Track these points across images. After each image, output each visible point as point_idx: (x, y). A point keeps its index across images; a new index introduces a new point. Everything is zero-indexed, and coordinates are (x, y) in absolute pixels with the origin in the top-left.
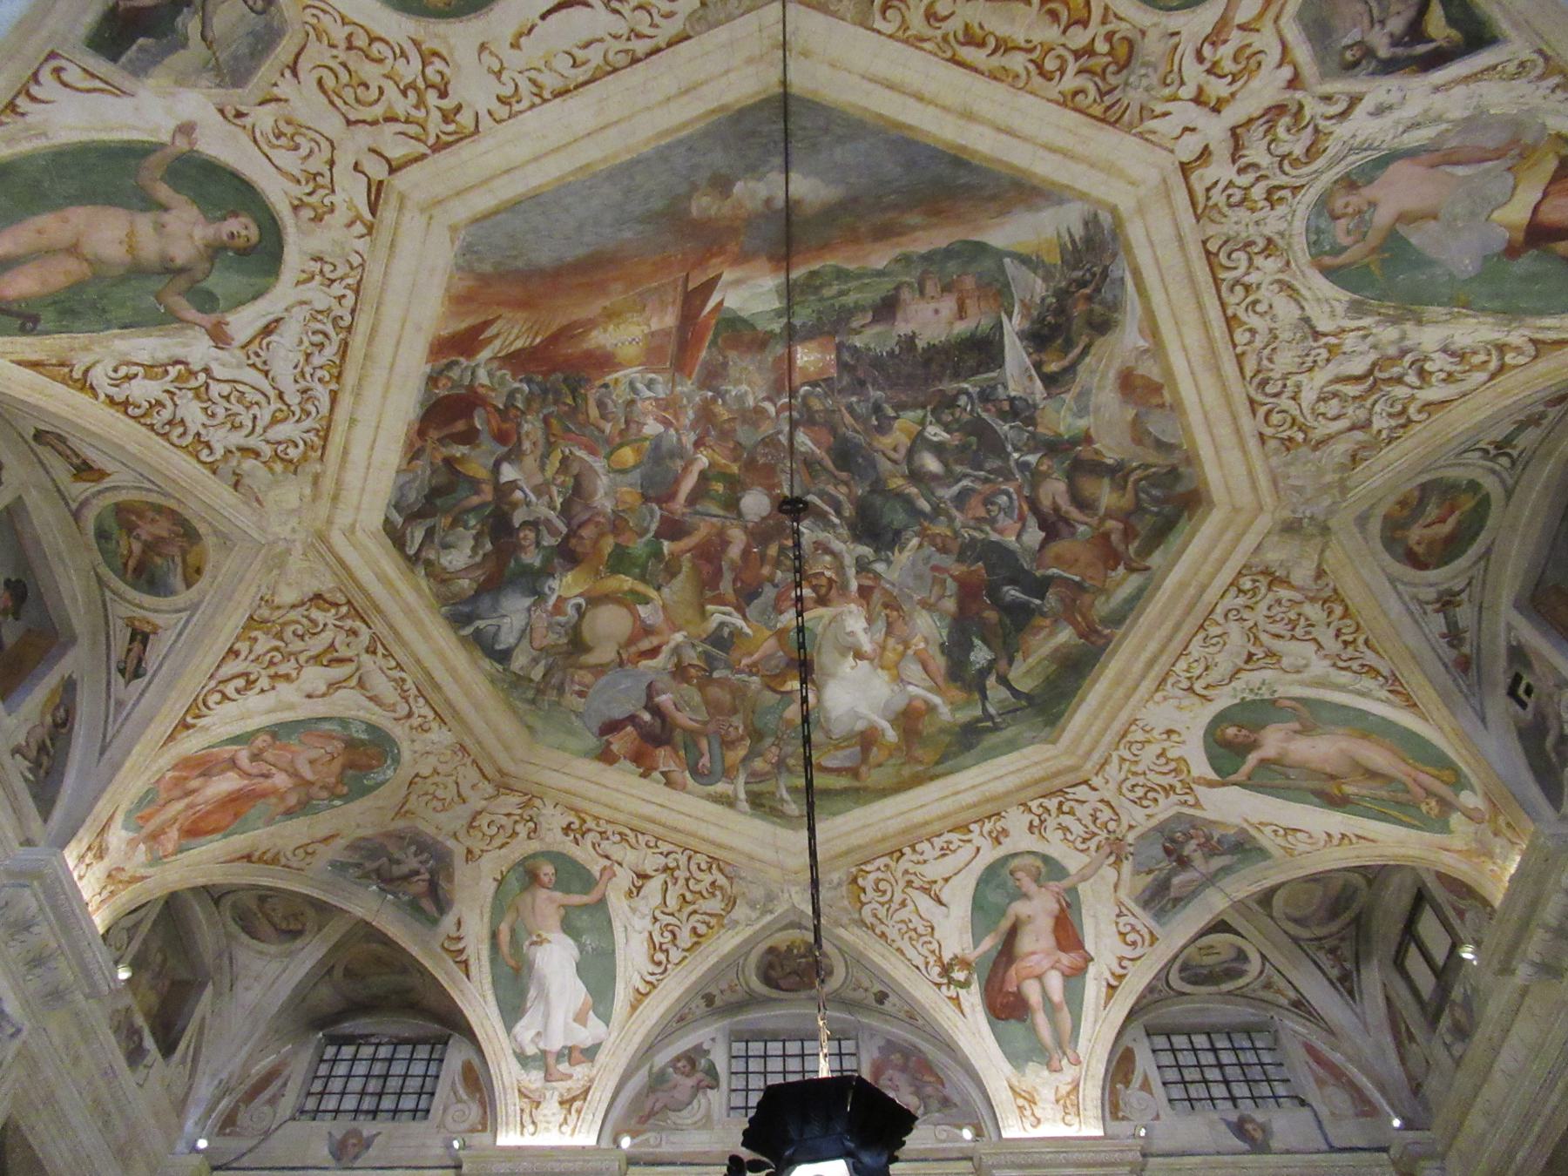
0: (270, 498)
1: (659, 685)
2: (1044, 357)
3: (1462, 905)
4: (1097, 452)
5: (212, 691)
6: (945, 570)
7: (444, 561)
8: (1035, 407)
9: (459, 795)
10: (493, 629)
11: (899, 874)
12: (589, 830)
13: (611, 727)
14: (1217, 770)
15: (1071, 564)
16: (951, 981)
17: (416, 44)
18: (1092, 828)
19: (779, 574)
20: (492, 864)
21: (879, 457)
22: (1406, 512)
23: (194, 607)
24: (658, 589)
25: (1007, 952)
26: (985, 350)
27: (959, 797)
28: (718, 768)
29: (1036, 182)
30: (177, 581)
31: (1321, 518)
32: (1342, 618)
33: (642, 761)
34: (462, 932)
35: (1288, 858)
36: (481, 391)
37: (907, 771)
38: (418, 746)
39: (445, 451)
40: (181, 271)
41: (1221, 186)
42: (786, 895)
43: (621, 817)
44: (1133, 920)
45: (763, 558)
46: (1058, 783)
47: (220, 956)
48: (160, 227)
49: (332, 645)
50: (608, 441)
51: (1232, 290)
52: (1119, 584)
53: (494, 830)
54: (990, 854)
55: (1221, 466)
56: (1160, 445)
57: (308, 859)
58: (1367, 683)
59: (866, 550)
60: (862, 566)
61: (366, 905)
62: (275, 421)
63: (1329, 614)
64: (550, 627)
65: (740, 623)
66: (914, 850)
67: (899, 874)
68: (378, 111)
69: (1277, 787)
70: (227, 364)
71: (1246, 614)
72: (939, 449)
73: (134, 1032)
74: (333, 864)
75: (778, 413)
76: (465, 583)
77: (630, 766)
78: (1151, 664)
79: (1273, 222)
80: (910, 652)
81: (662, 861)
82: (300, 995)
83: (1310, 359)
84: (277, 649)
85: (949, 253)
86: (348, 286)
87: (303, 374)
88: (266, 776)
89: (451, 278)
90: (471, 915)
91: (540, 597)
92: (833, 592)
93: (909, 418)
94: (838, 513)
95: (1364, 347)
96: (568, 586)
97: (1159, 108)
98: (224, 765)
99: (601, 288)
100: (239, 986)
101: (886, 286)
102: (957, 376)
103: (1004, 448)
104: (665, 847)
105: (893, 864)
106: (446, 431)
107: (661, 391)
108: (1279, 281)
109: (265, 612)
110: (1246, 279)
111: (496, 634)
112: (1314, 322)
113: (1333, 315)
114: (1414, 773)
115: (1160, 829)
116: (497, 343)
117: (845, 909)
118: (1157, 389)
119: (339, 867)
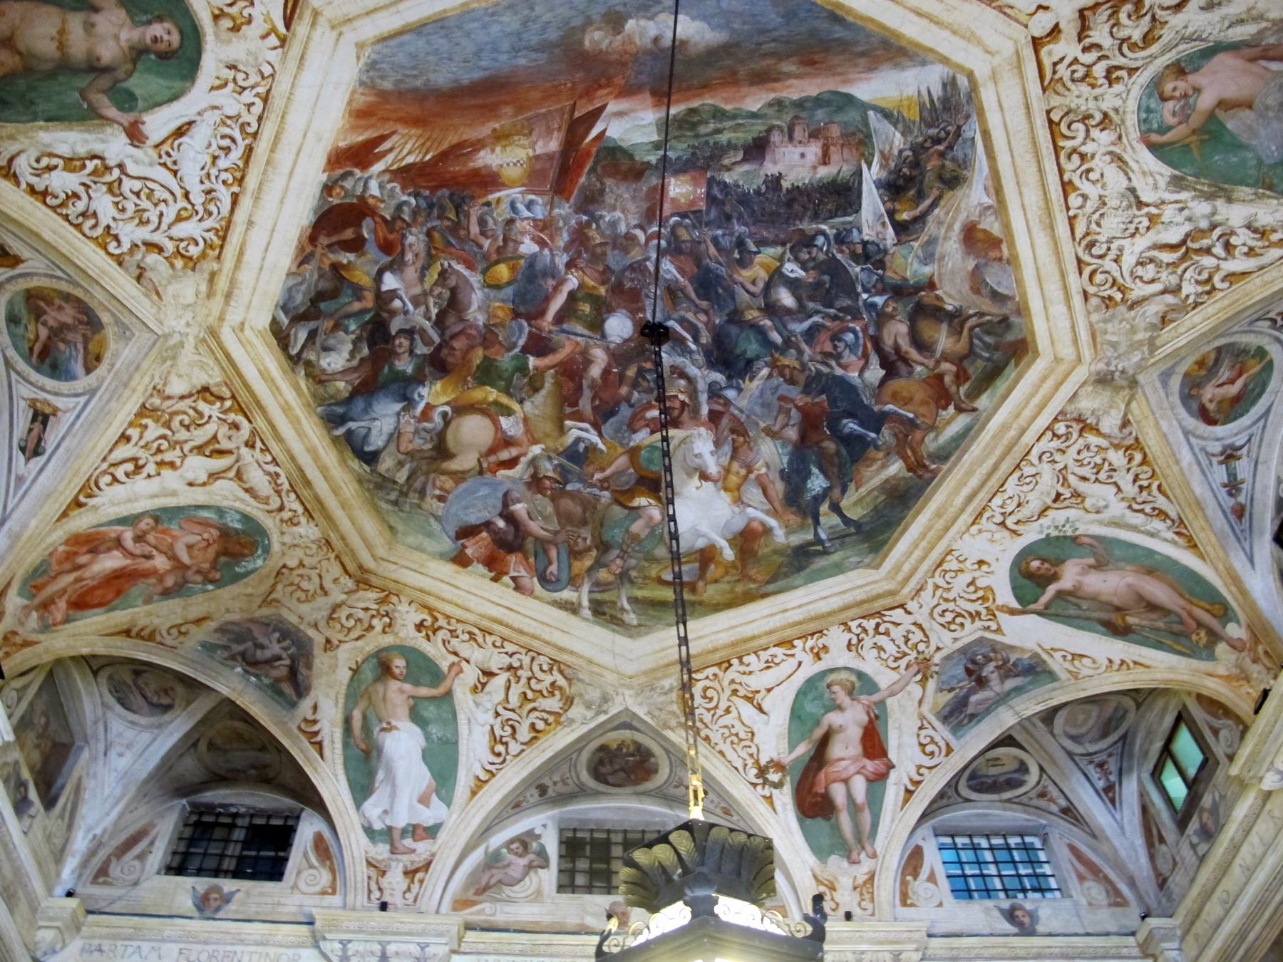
0: (169, 291)
1: (515, 495)
2: (898, 206)
3: (1217, 723)
4: (938, 298)
5: (105, 472)
6: (792, 401)
7: (323, 363)
8: (886, 252)
9: (322, 587)
10: (364, 431)
11: (725, 683)
12: (440, 628)
15: (907, 402)
16: (766, 782)
18: (904, 648)
19: (636, 394)
20: (348, 654)
21: (738, 288)
22: (1203, 373)
23: (92, 392)
24: (521, 402)
26: (843, 195)
28: (565, 577)
29: (904, 43)
30: (78, 368)
31: (1131, 372)
32: (1141, 464)
33: (495, 567)
34: (318, 716)
36: (371, 201)
37: (739, 588)
38: (287, 539)
39: (333, 257)
41: (1066, 62)
42: (620, 698)
44: (930, 732)
45: (621, 378)
46: (877, 605)
47: (96, 723)
49: (215, 437)
50: (486, 257)
51: (1069, 157)
52: (949, 422)
53: (352, 622)
54: (811, 668)
56: (996, 296)
57: (182, 639)
58: (1157, 525)
59: (718, 377)
61: (232, 685)
62: (179, 219)
63: (1130, 460)
64: (416, 432)
65: (593, 437)
67: (725, 683)
69: (1069, 617)
70: (140, 162)
71: (1058, 457)
72: (793, 285)
73: (22, 784)
74: (204, 645)
75: (648, 239)
76: (341, 385)
77: (481, 569)
78: (970, 499)
79: (1110, 99)
80: (752, 476)
81: (506, 660)
82: (167, 764)
83: (1132, 227)
84: (164, 437)
85: (818, 101)
86: (258, 95)
87: (208, 175)
88: (148, 557)
89: (354, 92)
90: (327, 701)
91: (409, 403)
92: (686, 414)
94: (696, 340)
95: (1180, 219)
96: (434, 394)
99: (490, 111)
100: (113, 754)
101: (758, 128)
102: (816, 217)
104: (510, 648)
105: (721, 674)
106: (334, 239)
107: (539, 212)
108: (1111, 153)
109: (156, 401)
110: (1083, 149)
111: (367, 436)
112: (1139, 193)
113: (1156, 187)
114: (1188, 606)
115: (963, 651)
116: (390, 158)
117: (673, 713)
118: (995, 243)
119: (209, 648)
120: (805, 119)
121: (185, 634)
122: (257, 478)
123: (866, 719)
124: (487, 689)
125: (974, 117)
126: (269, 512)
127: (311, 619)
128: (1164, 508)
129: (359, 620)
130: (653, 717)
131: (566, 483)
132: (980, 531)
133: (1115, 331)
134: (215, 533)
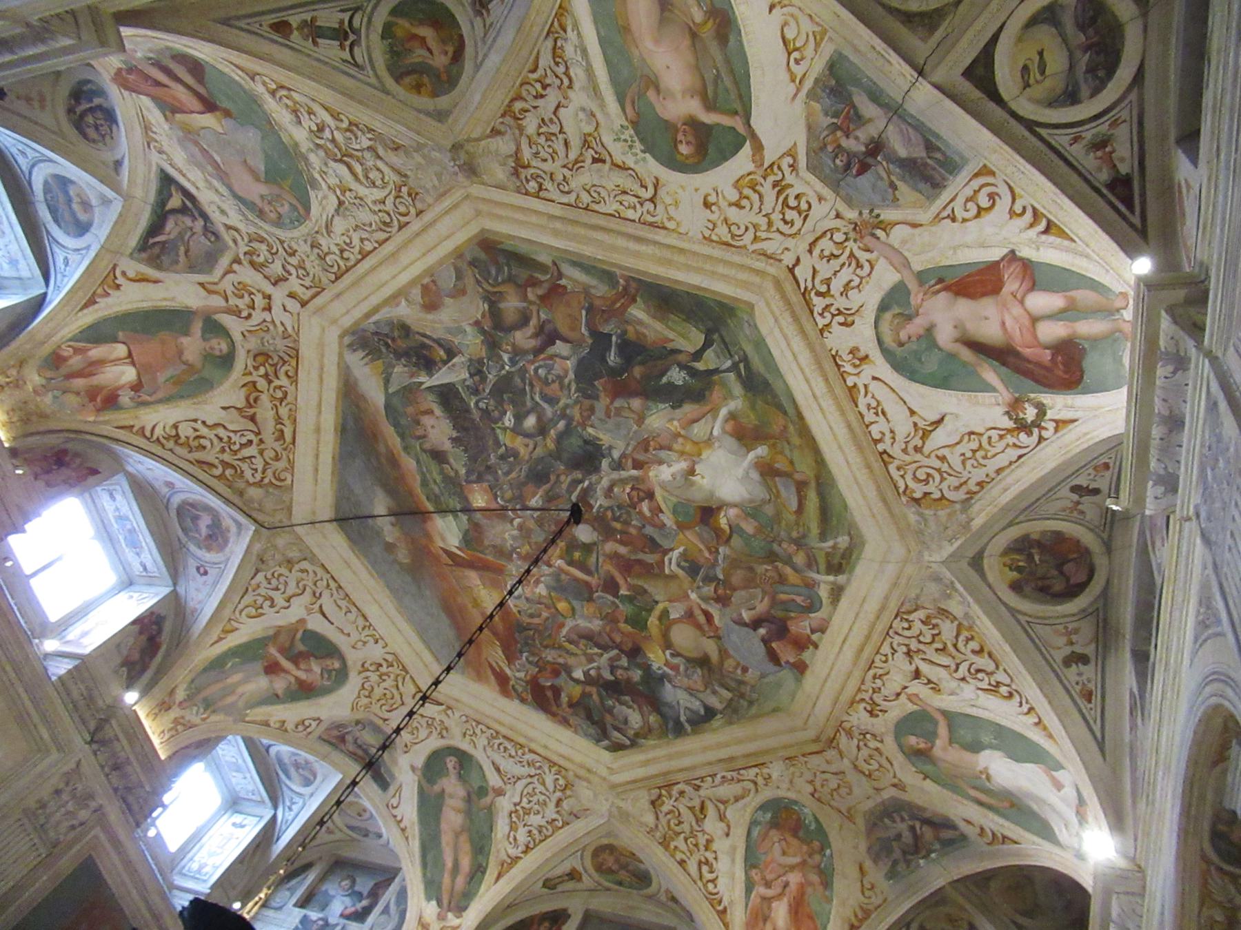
1: (735, 615)
4: (483, 316)
5: (705, 885)
6: (608, 407)
7: (637, 726)
8: (470, 360)
9: (836, 774)
11: (908, 459)
12: (871, 699)
13: (773, 657)
14: (738, 147)
16: (1036, 423)
17: (360, 673)
18: (844, 258)
20: (907, 773)
21: (535, 455)
22: (426, 79)
24: (657, 602)
25: (1002, 355)
26: (447, 395)
27: (818, 393)
28: (804, 591)
31: (449, 154)
33: (801, 644)
35: (830, 33)
37: (796, 440)
38: (785, 786)
39: (565, 706)
40: (469, 795)
43: (857, 674)
44: (958, 206)
45: (622, 532)
46: (796, 299)
48: (451, 796)
49: (690, 808)
51: (347, 259)
52: (575, 281)
53: (872, 762)
55: (453, 234)
56: (459, 276)
59: (605, 464)
60: (618, 466)
62: (544, 784)
64: (688, 677)
66: (880, 441)
67: (908, 459)
68: (395, 691)
69: (736, 83)
72: (519, 418)
77: (806, 656)
78: (639, 239)
79: (303, 248)
80: (682, 432)
81: (900, 656)
83: (357, 201)
85: (396, 425)
88: (786, 885)
91: (662, 678)
93: (506, 439)
94: (581, 481)
96: (657, 658)
97: (281, 329)
98: (765, 906)
101: (424, 457)
102: (468, 411)
103: (504, 376)
104: (886, 649)
105: (896, 463)
109: (658, 834)
113: (325, 197)
115: (835, 186)
118: (425, 289)
120: (409, 430)
121: (873, 887)
122: (725, 791)
123: (943, 295)
124: (935, 680)
125: (365, 325)
126: (757, 791)
127: (871, 792)
128: (550, 56)
129: (871, 756)
130: (955, 538)
131: (715, 578)
132: (670, 219)
133: (427, 180)
134: (775, 835)
